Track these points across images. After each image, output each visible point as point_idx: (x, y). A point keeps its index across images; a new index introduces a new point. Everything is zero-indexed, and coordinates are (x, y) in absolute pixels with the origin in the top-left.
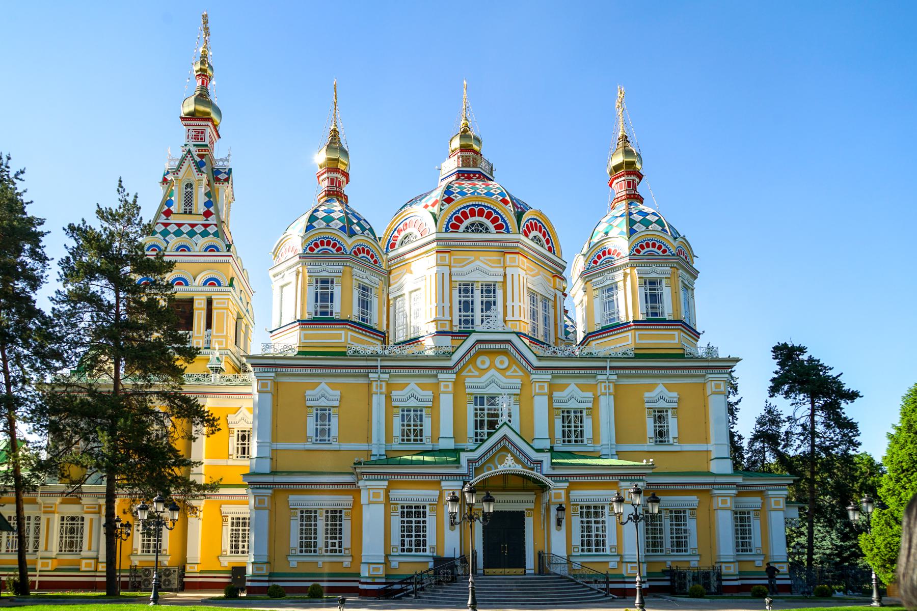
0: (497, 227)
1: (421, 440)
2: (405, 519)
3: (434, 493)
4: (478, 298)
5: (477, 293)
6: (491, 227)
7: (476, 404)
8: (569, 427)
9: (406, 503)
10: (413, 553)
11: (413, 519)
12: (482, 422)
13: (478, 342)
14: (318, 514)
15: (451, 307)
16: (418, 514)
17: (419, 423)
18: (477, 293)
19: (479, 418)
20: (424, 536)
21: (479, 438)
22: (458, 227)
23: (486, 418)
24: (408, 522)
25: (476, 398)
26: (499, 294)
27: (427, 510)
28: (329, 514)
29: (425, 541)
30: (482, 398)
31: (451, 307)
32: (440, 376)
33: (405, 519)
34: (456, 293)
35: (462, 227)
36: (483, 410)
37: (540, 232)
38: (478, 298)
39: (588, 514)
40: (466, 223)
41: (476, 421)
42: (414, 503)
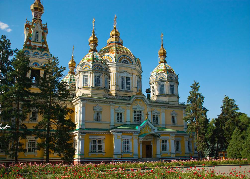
0: (130, 62)
1: (122, 121)
2: (125, 143)
3: (131, 137)
5: (125, 80)
7: (134, 113)
8: (155, 120)
9: (125, 139)
10: (126, 152)
11: (126, 143)
12: (136, 117)
13: (136, 97)
14: (96, 141)
16: (127, 142)
17: (121, 117)
18: (125, 80)
19: (135, 116)
20: (129, 147)
21: (135, 121)
23: (137, 116)
24: (125, 144)
25: (134, 111)
26: (131, 80)
28: (99, 141)
29: (129, 149)
30: (136, 111)
33: (125, 143)
36: (136, 114)
41: (134, 117)
42: (126, 139)
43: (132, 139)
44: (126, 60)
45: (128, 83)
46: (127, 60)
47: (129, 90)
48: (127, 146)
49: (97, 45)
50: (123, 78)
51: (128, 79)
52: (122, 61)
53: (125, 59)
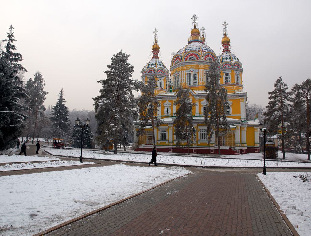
3: (167, 127)
4: (192, 77)
5: (192, 76)
6: (196, 58)
15: (185, 80)
18: (192, 76)
22: (187, 59)
26: (197, 75)
27: (166, 131)
31: (185, 80)
32: (173, 99)
34: (187, 76)
35: (188, 59)
37: (210, 56)
38: (192, 77)
39: (202, 132)
40: (189, 57)
42: (163, 129)
43: (168, 130)
44: (193, 57)
45: (195, 79)
46: (193, 56)
47: (196, 85)
48: (164, 135)
49: (159, 52)
50: (189, 75)
51: (195, 74)
52: (188, 59)
53: (192, 56)
